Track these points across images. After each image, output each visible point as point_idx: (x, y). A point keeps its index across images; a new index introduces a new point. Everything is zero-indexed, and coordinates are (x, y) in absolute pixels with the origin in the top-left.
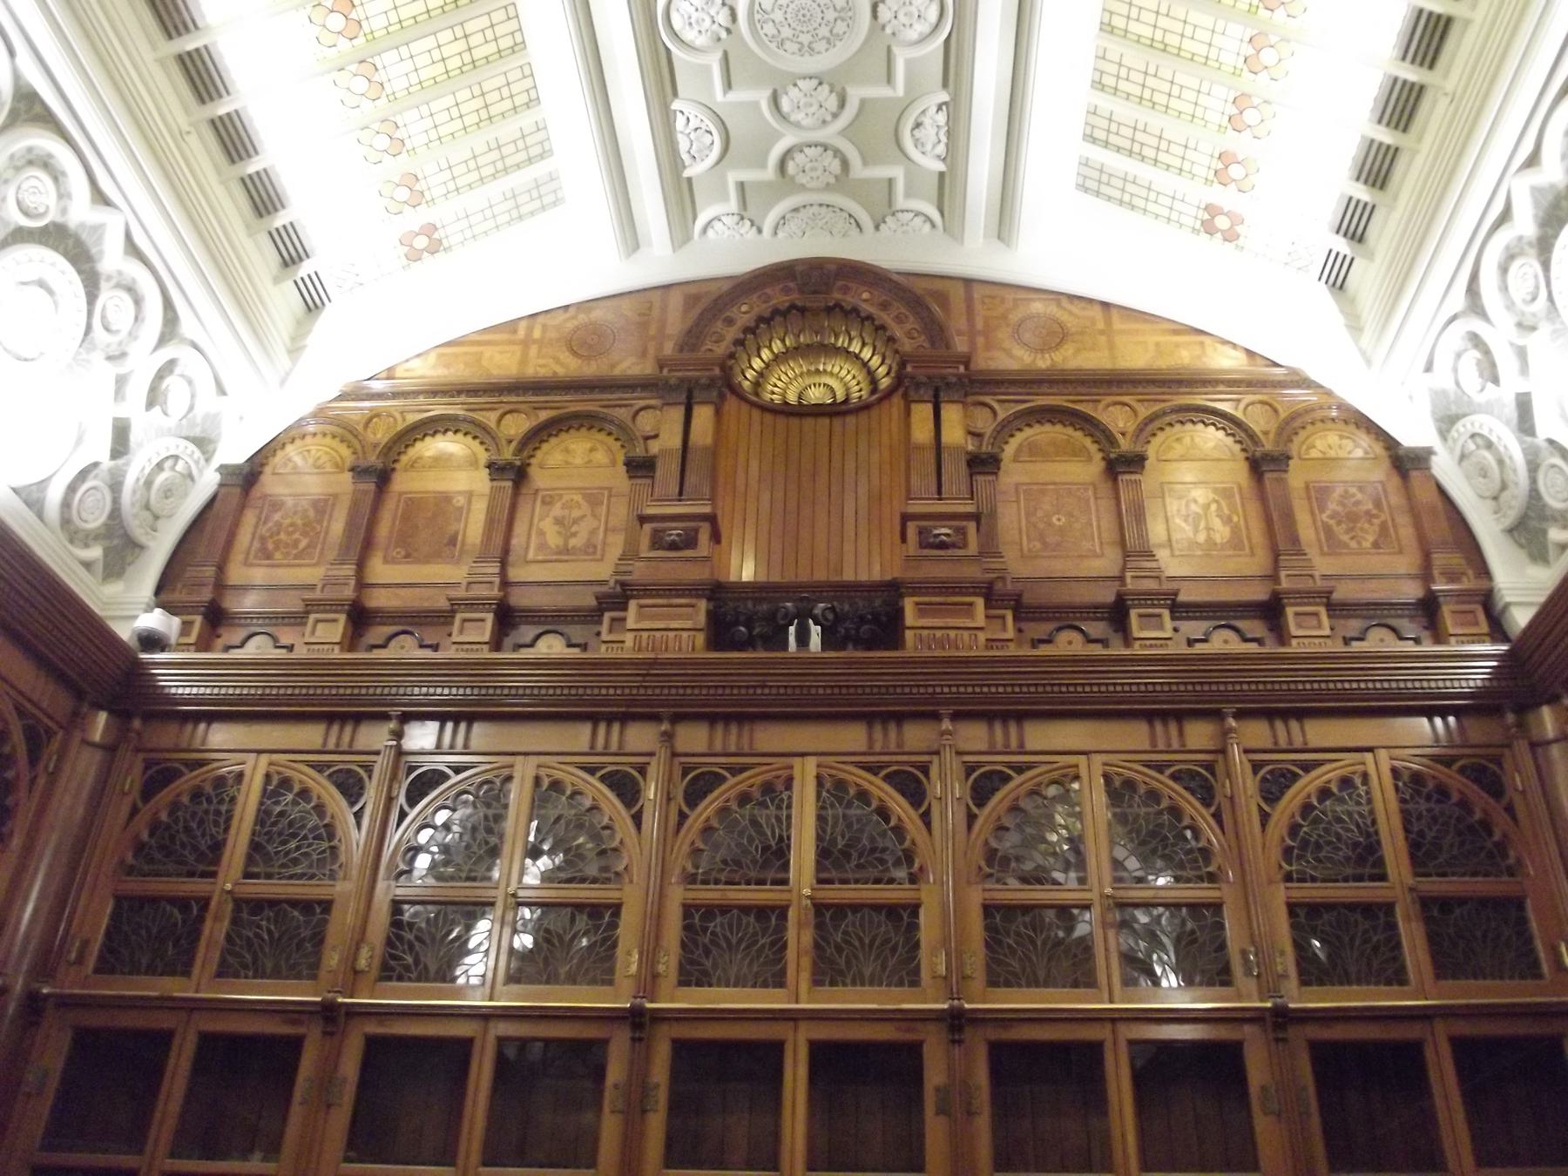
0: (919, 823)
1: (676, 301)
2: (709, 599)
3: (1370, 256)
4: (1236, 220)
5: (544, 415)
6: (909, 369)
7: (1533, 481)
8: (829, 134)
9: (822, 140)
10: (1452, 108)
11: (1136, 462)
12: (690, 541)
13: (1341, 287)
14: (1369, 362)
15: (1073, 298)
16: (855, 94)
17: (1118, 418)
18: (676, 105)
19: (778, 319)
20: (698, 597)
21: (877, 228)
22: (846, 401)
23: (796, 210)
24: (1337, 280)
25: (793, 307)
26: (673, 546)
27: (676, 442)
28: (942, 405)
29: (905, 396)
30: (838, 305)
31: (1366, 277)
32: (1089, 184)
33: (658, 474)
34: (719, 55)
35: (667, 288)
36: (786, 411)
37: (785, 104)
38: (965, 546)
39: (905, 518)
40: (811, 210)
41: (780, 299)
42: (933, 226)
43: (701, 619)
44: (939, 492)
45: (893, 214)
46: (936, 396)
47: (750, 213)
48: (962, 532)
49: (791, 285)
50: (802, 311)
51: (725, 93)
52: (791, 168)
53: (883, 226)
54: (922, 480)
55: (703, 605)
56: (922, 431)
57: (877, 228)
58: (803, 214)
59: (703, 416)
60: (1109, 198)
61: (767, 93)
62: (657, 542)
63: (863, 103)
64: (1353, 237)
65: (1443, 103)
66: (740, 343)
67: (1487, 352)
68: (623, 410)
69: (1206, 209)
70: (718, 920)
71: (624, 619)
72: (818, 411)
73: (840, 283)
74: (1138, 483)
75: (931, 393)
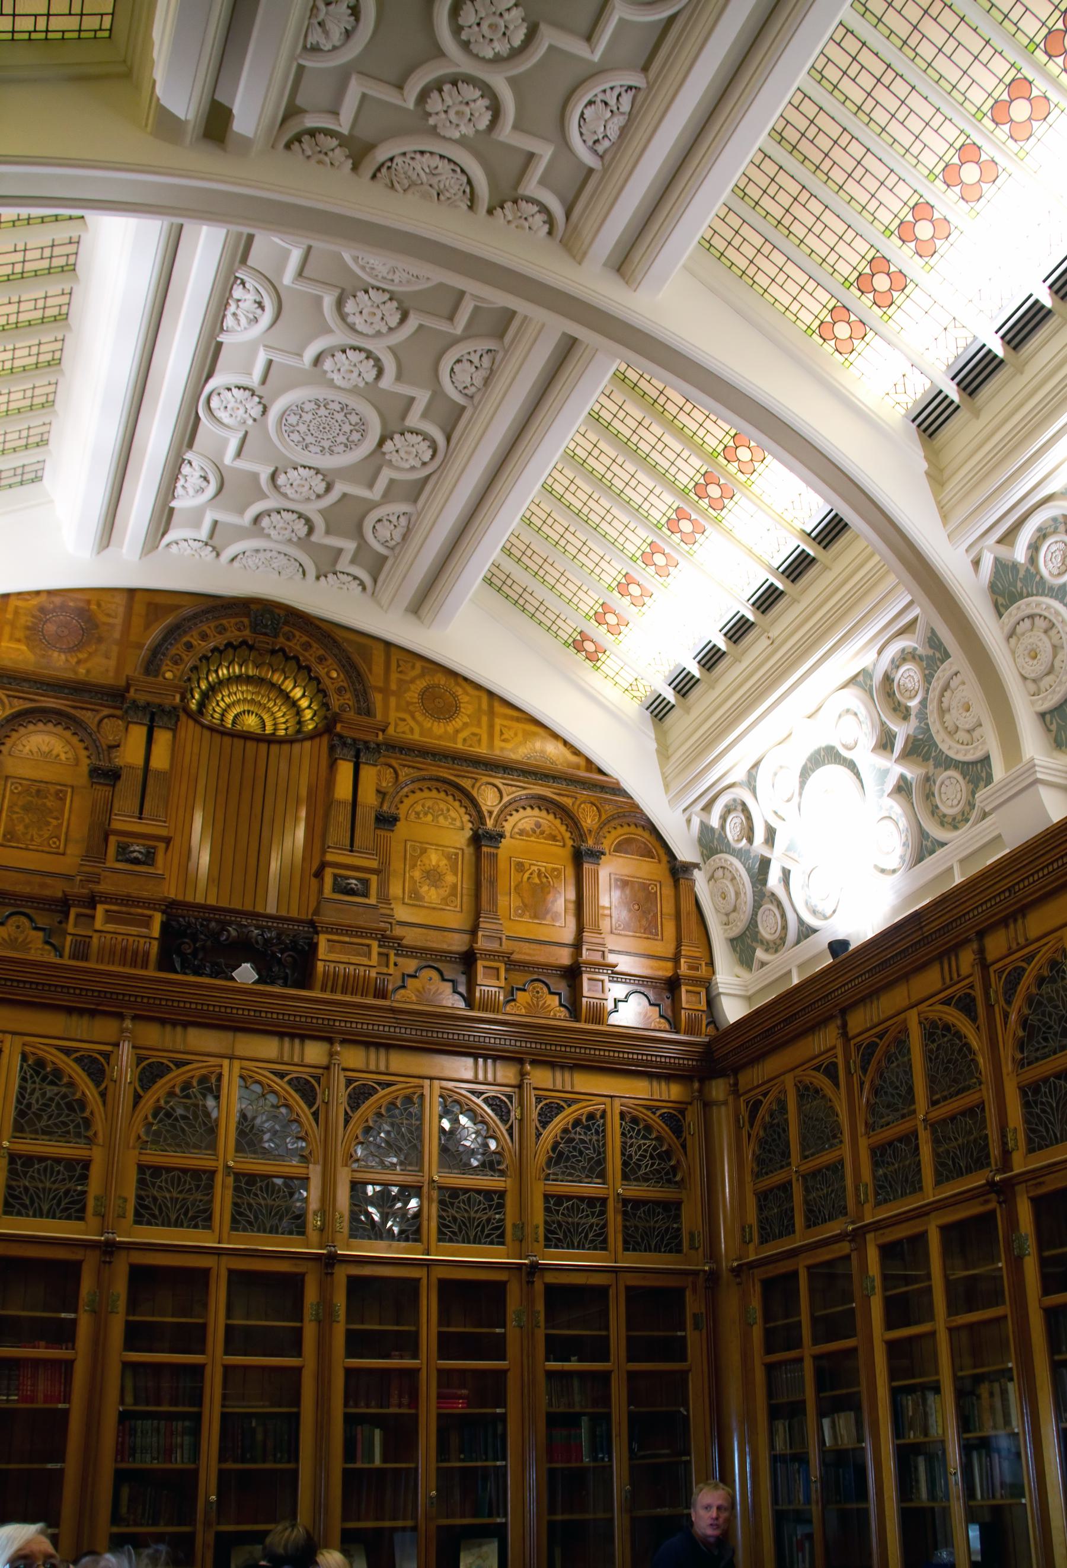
0: (311, 1117)
1: (139, 608)
2: (163, 912)
3: (688, 710)
4: (600, 650)
5: (20, 705)
6: (339, 728)
7: (755, 914)
8: (311, 510)
9: (302, 511)
10: (770, 649)
11: (496, 838)
12: (149, 858)
13: (660, 719)
14: (667, 786)
15: (466, 679)
16: (339, 488)
17: (489, 799)
18: (188, 456)
19: (230, 651)
20: (155, 910)
21: (318, 578)
22: (273, 734)
23: (257, 551)
24: (659, 710)
25: (244, 643)
26: (136, 861)
27: (138, 760)
28: (362, 766)
29: (332, 748)
30: (282, 650)
31: (678, 722)
32: (495, 580)
33: (120, 785)
34: (241, 434)
35: (131, 592)
36: (218, 731)
37: (281, 480)
38: (366, 895)
39: (323, 865)
40: (268, 554)
41: (233, 635)
42: (364, 589)
43: (156, 931)
44: (352, 845)
45: (335, 573)
46: (357, 756)
47: (216, 541)
48: (366, 883)
49: (246, 621)
50: (251, 648)
51: (234, 459)
52: (265, 522)
53: (323, 579)
54: (338, 833)
55: (158, 918)
56: (343, 790)
57: (318, 578)
58: (261, 555)
59: (163, 738)
60: (507, 597)
61: (271, 469)
62: (123, 852)
63: (345, 495)
64: (679, 692)
65: (764, 643)
66: (195, 669)
67: (749, 818)
68: (89, 713)
69: (581, 633)
70: (163, 1177)
71: (93, 917)
72: (247, 736)
73: (286, 629)
74: (494, 857)
75: (352, 753)
